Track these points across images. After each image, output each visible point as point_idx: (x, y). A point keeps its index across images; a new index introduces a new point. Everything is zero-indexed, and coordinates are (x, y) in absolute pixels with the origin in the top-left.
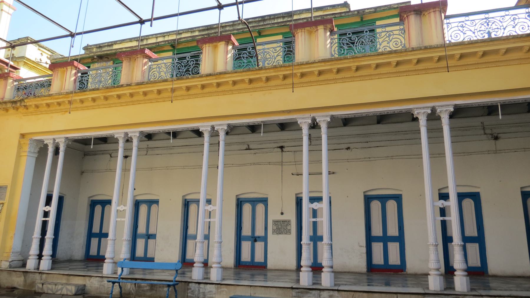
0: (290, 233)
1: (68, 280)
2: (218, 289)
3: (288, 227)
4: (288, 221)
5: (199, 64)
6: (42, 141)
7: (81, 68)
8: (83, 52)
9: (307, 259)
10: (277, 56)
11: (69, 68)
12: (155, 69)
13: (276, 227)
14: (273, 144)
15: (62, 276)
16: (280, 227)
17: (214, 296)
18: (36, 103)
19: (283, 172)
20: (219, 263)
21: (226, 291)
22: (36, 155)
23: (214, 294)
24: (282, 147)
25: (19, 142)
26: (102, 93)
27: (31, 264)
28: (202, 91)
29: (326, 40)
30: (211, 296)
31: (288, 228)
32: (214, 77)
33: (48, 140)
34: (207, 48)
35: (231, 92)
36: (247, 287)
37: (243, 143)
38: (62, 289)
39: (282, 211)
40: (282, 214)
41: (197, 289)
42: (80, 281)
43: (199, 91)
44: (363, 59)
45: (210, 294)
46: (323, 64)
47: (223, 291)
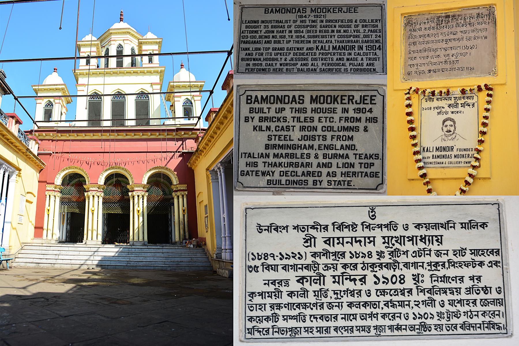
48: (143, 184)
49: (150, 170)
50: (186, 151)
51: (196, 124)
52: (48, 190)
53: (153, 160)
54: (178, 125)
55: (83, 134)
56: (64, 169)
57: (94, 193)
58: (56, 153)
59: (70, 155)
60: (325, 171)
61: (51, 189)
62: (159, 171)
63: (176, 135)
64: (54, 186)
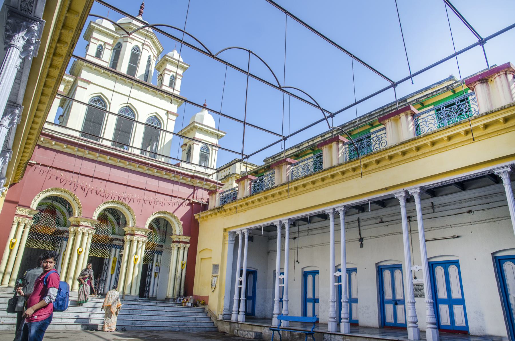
0: (423, 296)
1: (252, 329)
5: (322, 162)
6: (235, 232)
7: (253, 179)
8: (264, 163)
9: (412, 316)
10: (375, 144)
11: (246, 180)
12: (295, 172)
15: (248, 325)
18: (229, 207)
19: (412, 240)
22: (234, 243)
25: (223, 234)
26: (263, 195)
27: (234, 318)
28: (323, 183)
29: (408, 124)
31: (422, 291)
32: (328, 171)
33: (238, 230)
34: (325, 149)
35: (343, 180)
36: (364, 339)
37: (377, 218)
38: (247, 334)
41: (329, 339)
42: (258, 330)
43: (321, 183)
44: (434, 135)
46: (403, 146)
48: (146, 229)
49: (156, 213)
50: (197, 201)
51: (210, 175)
52: (18, 215)
53: (161, 203)
54: (194, 171)
55: (87, 152)
56: (48, 190)
57: (85, 230)
58: (42, 165)
59: (62, 173)
61: (24, 214)
62: (163, 217)
63: (190, 181)
64: (30, 210)
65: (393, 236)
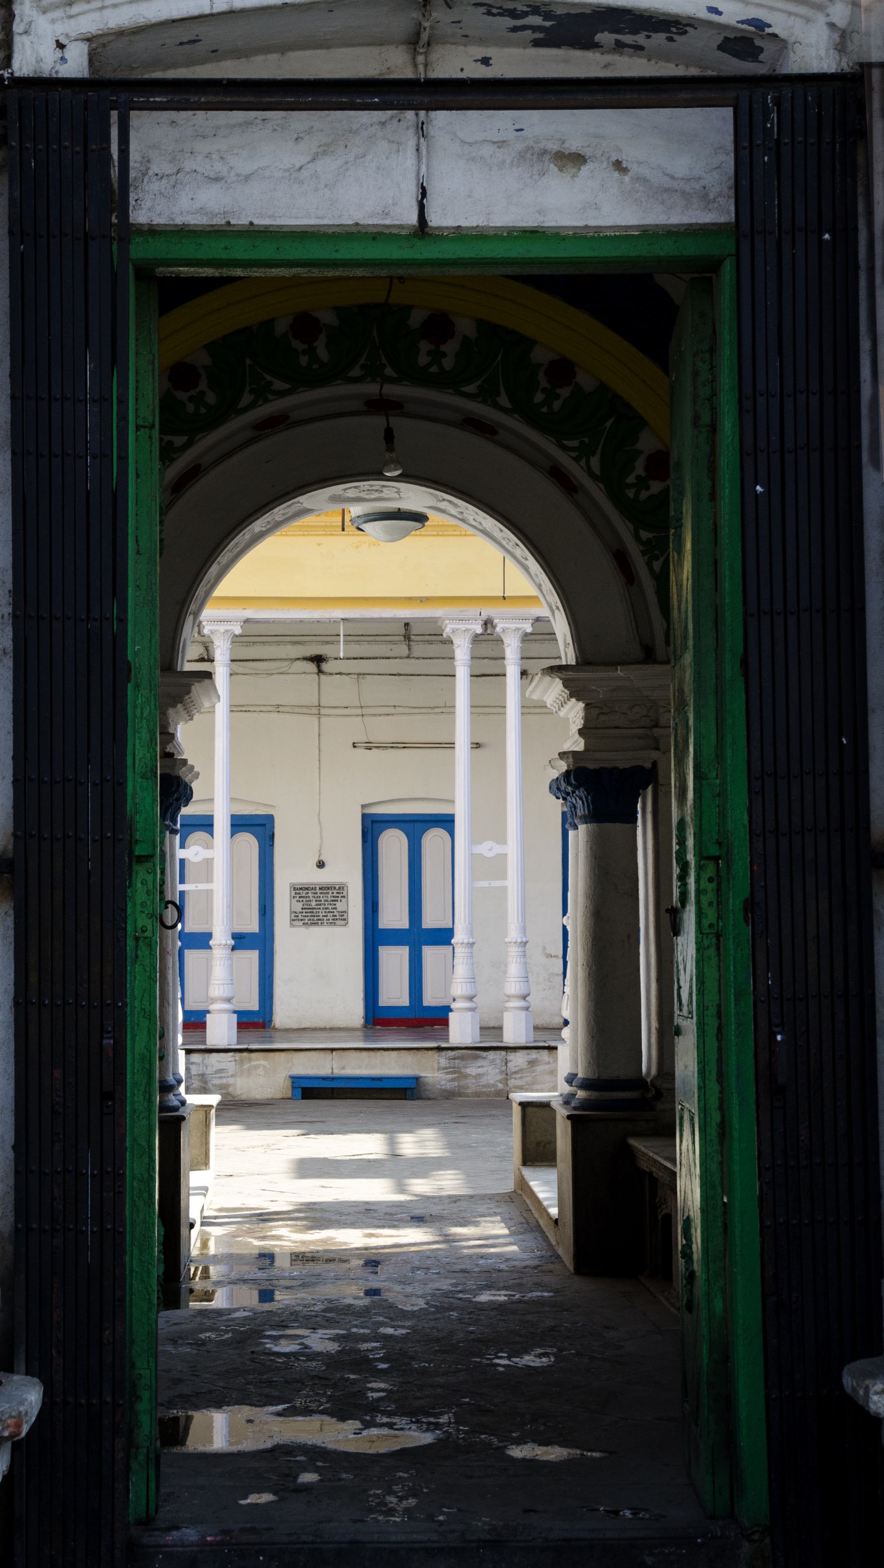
0: (343, 922)
2: (242, 1061)
3: (338, 904)
4: (339, 888)
13: (300, 905)
14: (289, 647)
16: (314, 903)
17: (231, 1081)
19: (322, 737)
20: (229, 1000)
21: (264, 1067)
23: (232, 1076)
24: (318, 660)
30: (224, 1081)
31: (340, 906)
36: (322, 1054)
39: (321, 858)
40: (321, 865)
45: (221, 1077)
47: (256, 1067)
60: (325, 918)
65: (249, 714)
